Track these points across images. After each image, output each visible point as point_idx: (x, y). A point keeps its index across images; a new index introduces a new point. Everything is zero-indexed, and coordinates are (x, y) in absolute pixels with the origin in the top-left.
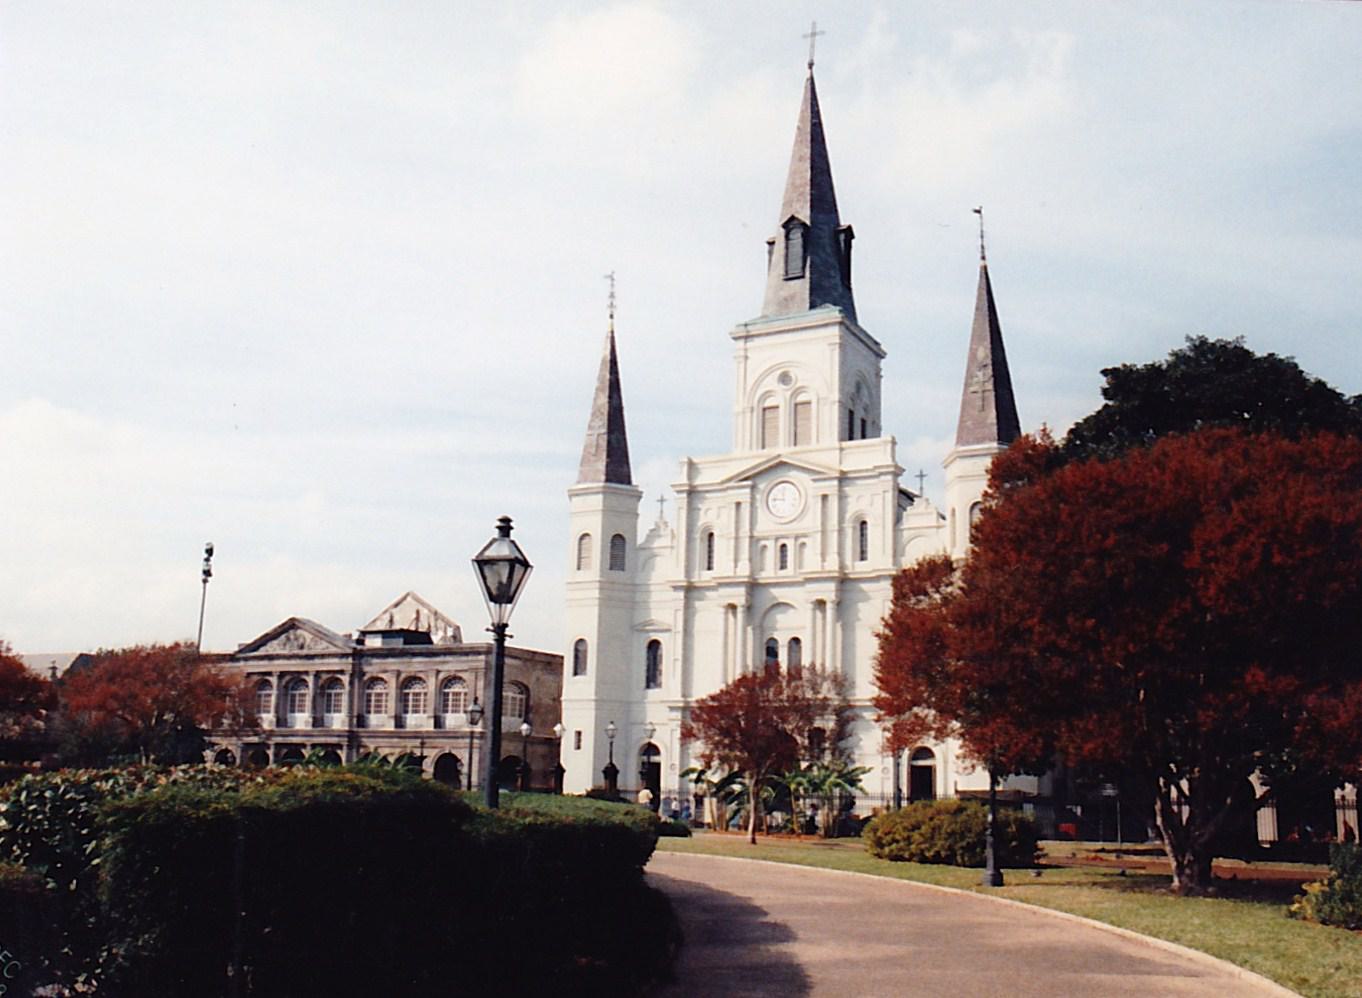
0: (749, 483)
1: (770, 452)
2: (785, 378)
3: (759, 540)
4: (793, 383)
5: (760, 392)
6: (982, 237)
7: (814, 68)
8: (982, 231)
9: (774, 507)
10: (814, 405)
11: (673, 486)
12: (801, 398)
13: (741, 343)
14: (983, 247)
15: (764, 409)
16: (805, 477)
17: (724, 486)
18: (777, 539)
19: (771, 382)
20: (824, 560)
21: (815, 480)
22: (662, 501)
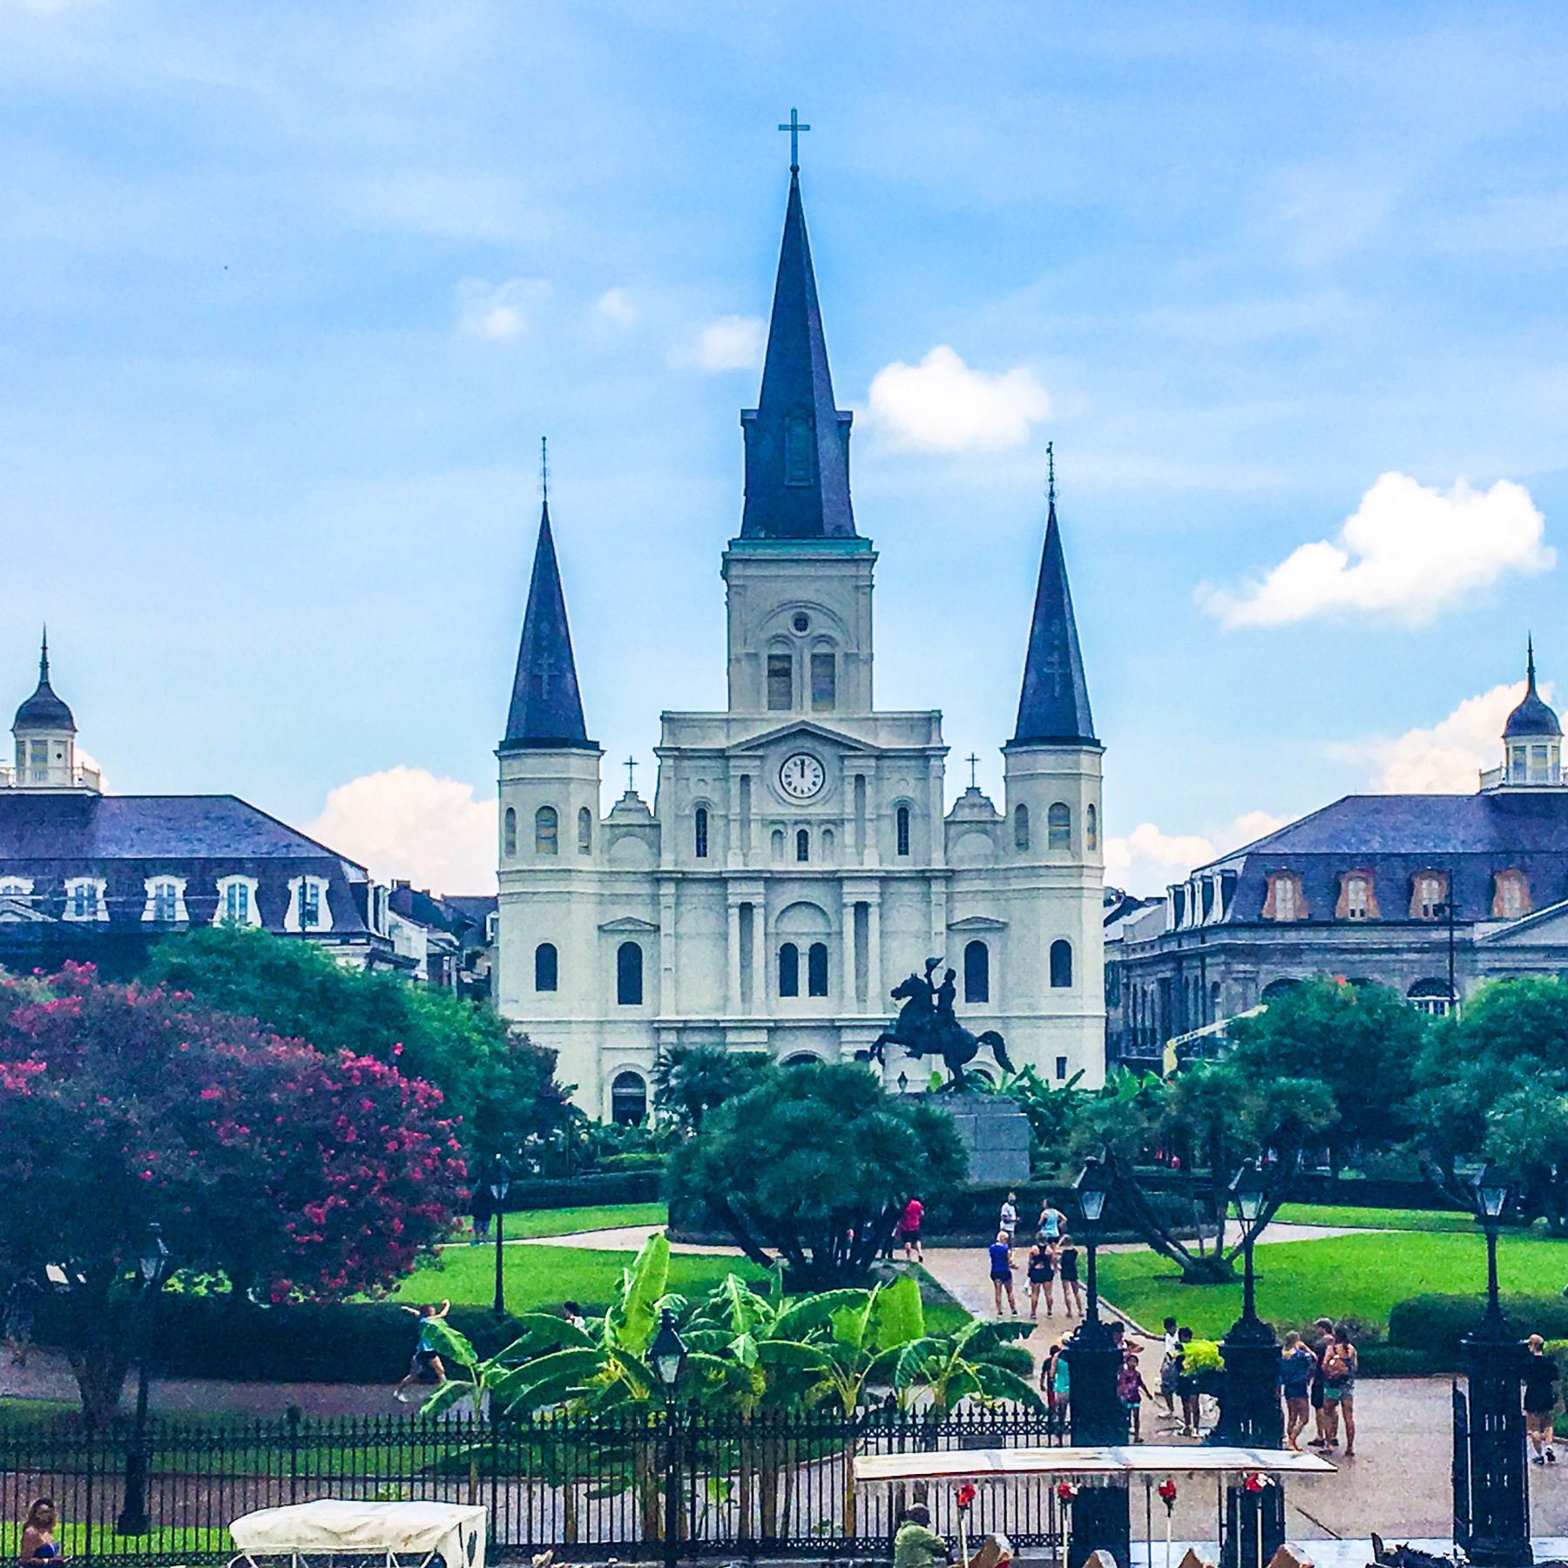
0: (760, 752)
1: (793, 717)
2: (801, 623)
3: (773, 822)
4: (808, 631)
5: (763, 636)
6: (1052, 480)
7: (799, 173)
8: (1051, 474)
9: (790, 784)
10: (839, 659)
11: (654, 750)
12: (823, 649)
13: (736, 570)
14: (1052, 494)
15: (770, 657)
16: (827, 752)
17: (722, 755)
18: (796, 823)
19: (785, 623)
20: (860, 854)
21: (842, 758)
22: (631, 764)
